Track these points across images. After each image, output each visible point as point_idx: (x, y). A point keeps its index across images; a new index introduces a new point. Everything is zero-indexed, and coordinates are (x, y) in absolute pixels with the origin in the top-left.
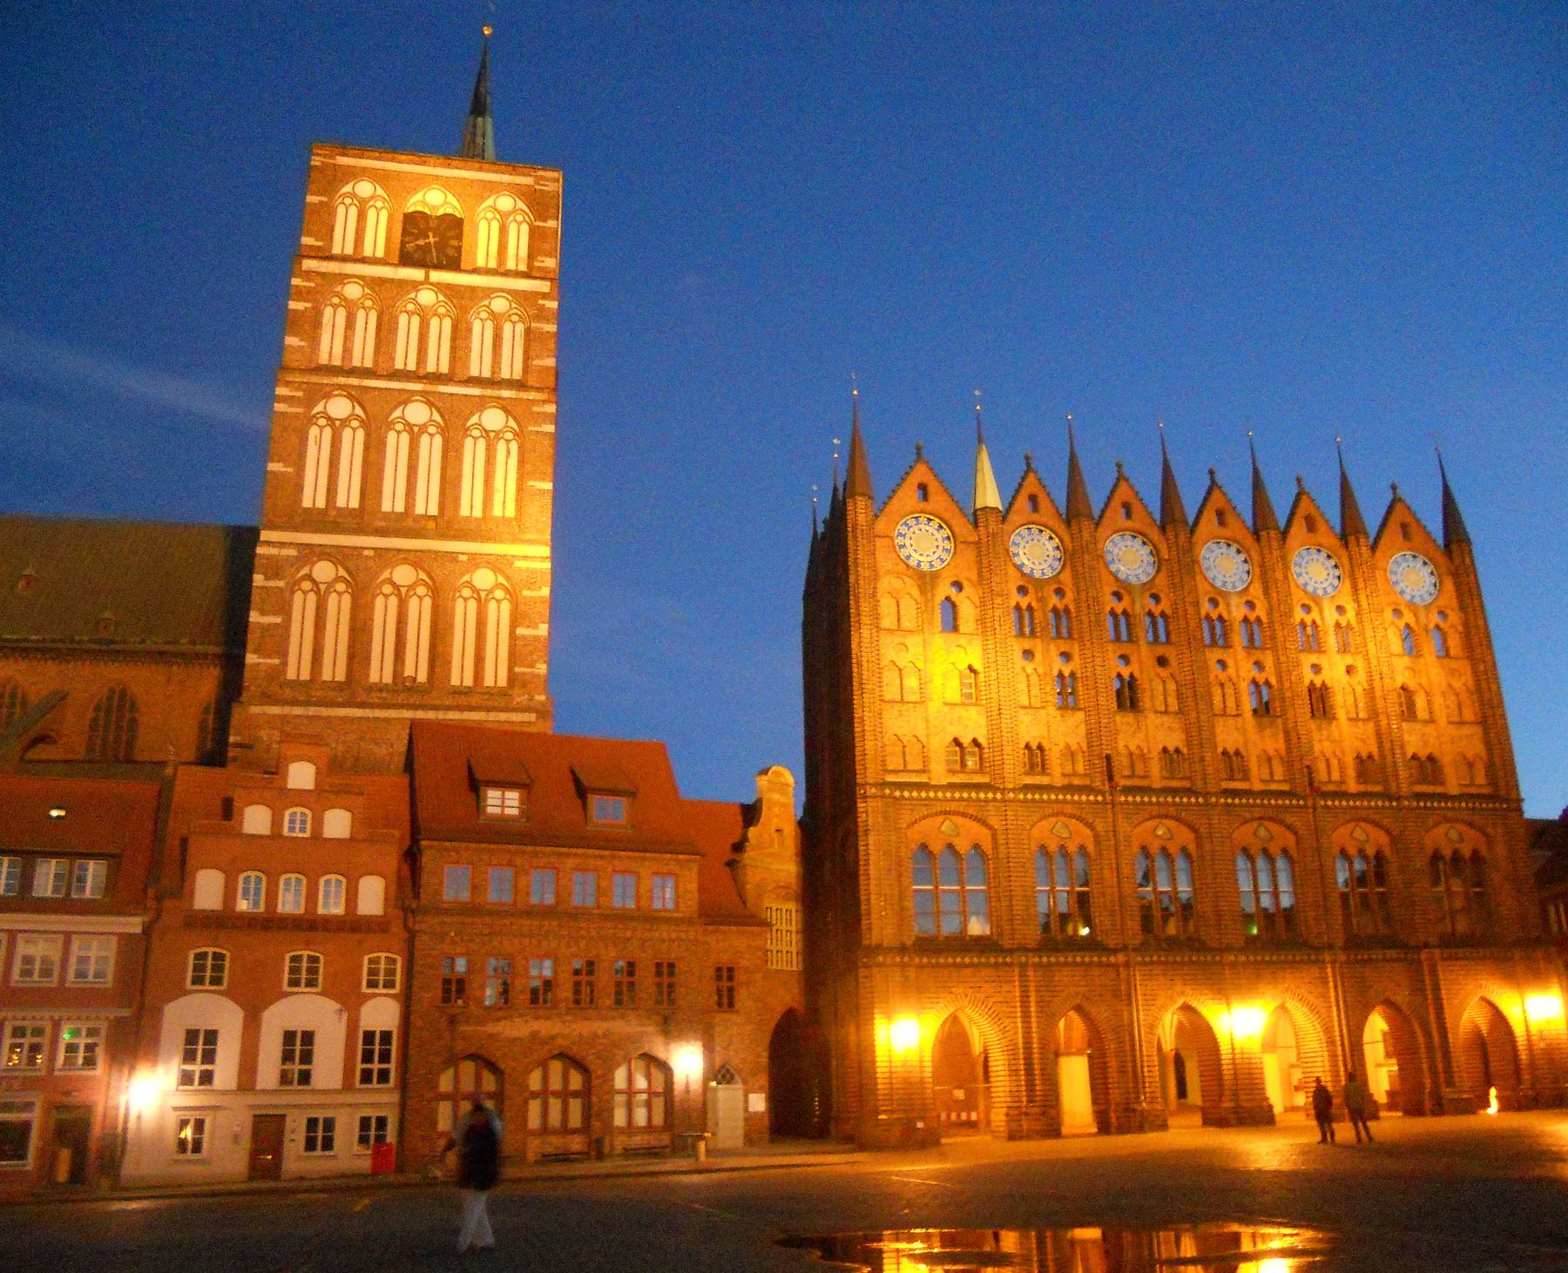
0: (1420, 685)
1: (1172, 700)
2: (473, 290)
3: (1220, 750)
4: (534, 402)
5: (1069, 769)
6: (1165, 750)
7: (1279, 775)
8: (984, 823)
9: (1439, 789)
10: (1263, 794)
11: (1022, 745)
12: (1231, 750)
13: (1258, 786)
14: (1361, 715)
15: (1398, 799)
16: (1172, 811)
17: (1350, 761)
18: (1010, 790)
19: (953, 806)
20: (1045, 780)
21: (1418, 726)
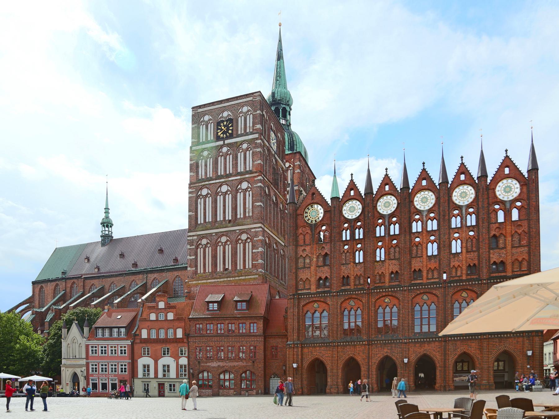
0: (502, 233)
1: (397, 254)
2: (236, 142)
3: (413, 270)
4: (255, 177)
5: (357, 282)
6: (392, 273)
7: (436, 276)
8: (326, 303)
9: (503, 274)
10: (427, 284)
11: (342, 276)
12: (417, 270)
13: (425, 281)
14: (474, 249)
15: (481, 281)
16: (390, 294)
17: (464, 267)
18: (334, 292)
19: (317, 299)
20: (348, 287)
21: (498, 250)
